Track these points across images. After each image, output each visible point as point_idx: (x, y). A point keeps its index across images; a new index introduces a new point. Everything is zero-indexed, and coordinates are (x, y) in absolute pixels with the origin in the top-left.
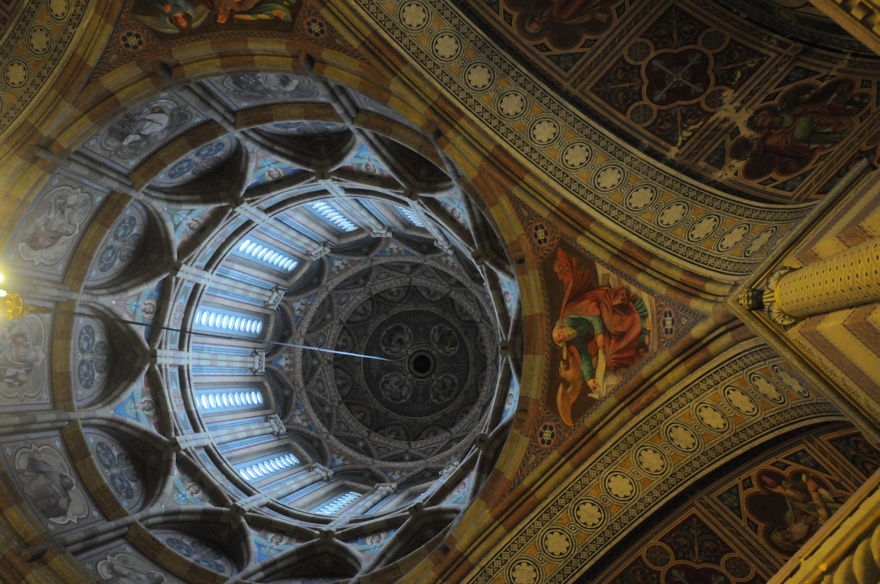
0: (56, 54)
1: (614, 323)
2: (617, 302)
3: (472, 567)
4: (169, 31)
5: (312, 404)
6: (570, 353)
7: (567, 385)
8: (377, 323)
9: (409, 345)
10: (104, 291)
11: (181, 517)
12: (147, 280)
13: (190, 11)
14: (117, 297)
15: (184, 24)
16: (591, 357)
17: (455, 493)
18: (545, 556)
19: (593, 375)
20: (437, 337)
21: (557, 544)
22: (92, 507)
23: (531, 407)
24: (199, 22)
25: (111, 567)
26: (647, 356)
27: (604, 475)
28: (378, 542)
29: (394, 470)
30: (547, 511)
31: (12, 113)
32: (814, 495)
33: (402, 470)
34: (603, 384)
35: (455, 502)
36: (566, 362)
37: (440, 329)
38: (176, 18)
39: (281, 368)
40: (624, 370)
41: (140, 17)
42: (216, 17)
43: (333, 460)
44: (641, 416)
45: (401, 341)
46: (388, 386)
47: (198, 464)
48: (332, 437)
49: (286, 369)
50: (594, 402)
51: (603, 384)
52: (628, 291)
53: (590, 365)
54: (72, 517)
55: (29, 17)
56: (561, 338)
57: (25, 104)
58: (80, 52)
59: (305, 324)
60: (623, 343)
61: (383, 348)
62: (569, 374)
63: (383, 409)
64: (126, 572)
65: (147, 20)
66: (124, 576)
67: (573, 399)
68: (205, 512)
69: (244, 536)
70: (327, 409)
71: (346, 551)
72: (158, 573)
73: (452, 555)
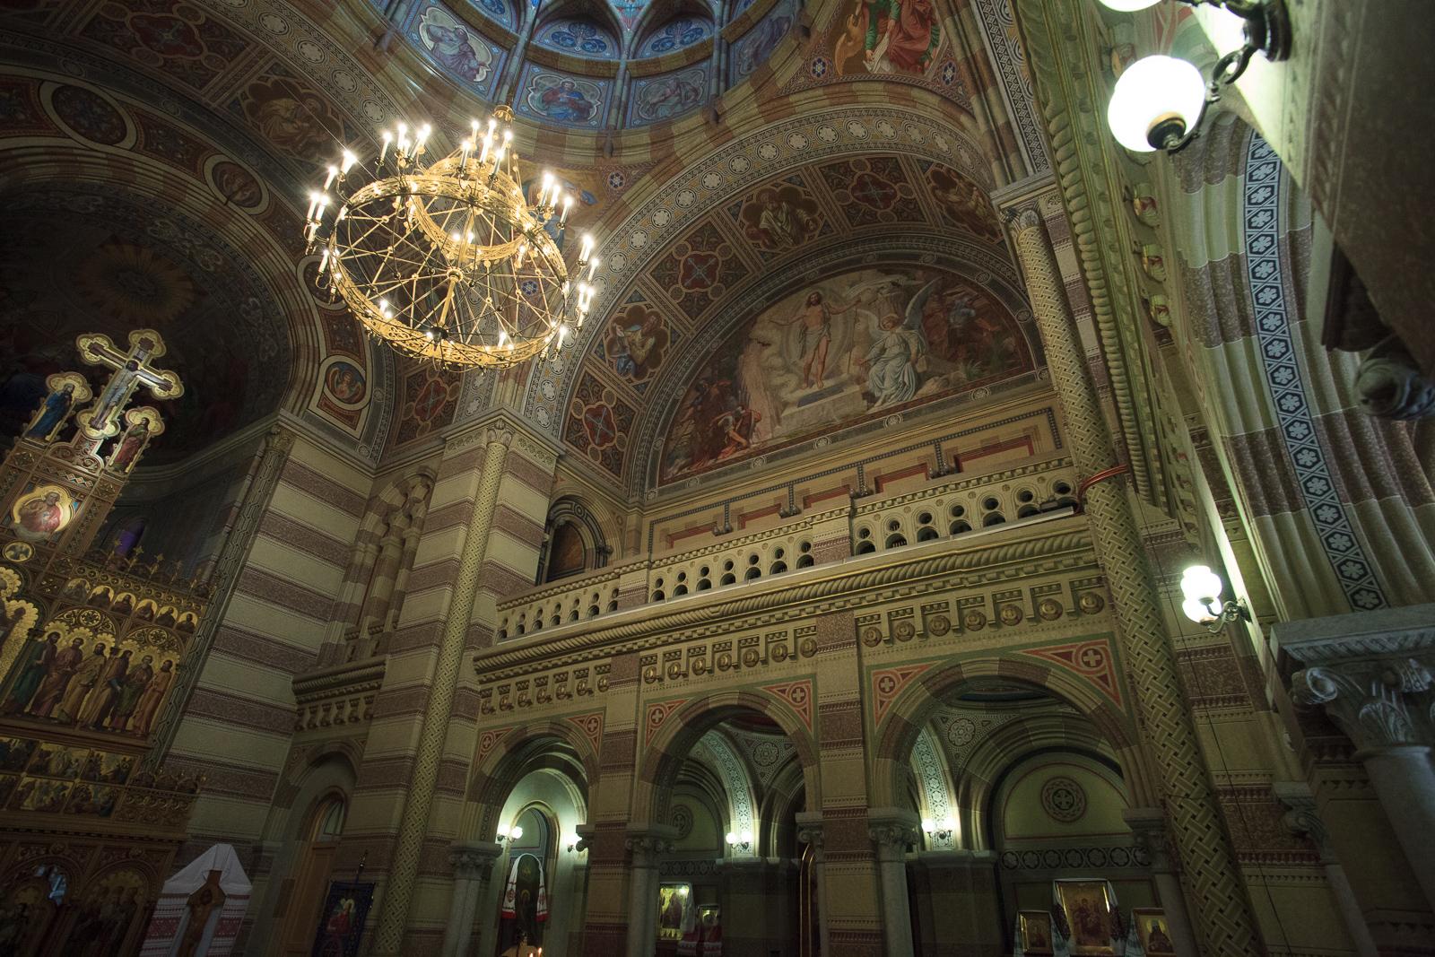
1: (909, 22)
2: (921, 8)
6: (862, 14)
16: (879, 32)
19: (873, 48)
21: (798, 142)
23: (814, 36)
25: (428, 31)
26: (919, 77)
32: (974, 197)
36: (856, 18)
44: (895, 107)
51: (877, 62)
52: (932, 11)
53: (875, 38)
60: (907, 45)
62: (855, 30)
64: (440, 34)
67: (850, 54)
72: (462, 28)
73: (721, 127)
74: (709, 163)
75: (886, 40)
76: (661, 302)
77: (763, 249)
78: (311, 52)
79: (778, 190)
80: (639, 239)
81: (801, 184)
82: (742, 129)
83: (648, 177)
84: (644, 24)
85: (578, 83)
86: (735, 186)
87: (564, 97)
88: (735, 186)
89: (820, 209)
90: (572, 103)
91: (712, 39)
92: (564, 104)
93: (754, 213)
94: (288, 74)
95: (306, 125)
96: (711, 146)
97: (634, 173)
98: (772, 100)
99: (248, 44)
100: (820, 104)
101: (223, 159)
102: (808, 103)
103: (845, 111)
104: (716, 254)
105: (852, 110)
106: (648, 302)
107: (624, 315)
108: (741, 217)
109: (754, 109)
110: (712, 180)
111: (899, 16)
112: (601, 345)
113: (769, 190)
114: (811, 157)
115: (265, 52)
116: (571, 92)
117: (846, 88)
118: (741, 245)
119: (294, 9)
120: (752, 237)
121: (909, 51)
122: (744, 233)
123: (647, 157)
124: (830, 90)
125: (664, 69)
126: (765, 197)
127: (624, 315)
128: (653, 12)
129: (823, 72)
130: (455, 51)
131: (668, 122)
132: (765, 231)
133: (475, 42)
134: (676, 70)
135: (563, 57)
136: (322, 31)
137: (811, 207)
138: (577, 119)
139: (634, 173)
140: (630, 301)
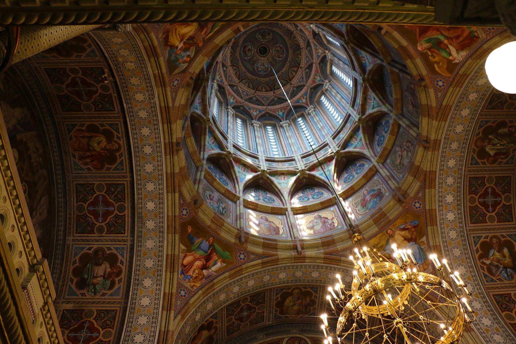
0: (154, 113)
3: (440, 140)
4: (185, 67)
5: (249, 102)
7: (438, 63)
8: (238, 53)
9: (253, 49)
10: (202, 153)
11: (292, 190)
12: (205, 134)
13: (188, 53)
14: (206, 150)
15: (188, 59)
17: (368, 104)
18: (463, 119)
19: (450, 54)
20: (260, 37)
21: (465, 112)
22: (277, 216)
23: (426, 78)
24: (193, 54)
27: (474, 82)
28: (356, 140)
29: (300, 99)
30: (457, 106)
31: (158, 145)
33: (302, 96)
34: (457, 56)
35: (373, 108)
36: (432, 56)
37: (259, 34)
38: (185, 61)
39: (233, 102)
40: (468, 48)
41: (173, 74)
42: (198, 46)
43: (279, 115)
45: (249, 50)
46: (259, 69)
47: (275, 169)
48: (269, 107)
49: (234, 101)
50: (457, 64)
51: (457, 56)
53: (447, 52)
54: (281, 227)
55: (131, 110)
56: (423, 49)
57: (159, 138)
58: (163, 105)
59: (224, 80)
60: (461, 39)
61: (246, 58)
62: (437, 59)
63: (267, 79)
65: (177, 71)
66: (313, 226)
67: (445, 66)
68: (295, 181)
69: (314, 176)
70: (254, 99)
71: (349, 152)
72: (316, 214)
73: (432, 142)
74: (443, 159)
75: (451, 47)
76: (490, 230)
77: (505, 161)
78: (282, 276)
79: (481, 135)
80: (451, 216)
81: (487, 122)
82: (440, 134)
83: (427, 190)
84: (368, 142)
85: (367, 187)
86: (462, 154)
87: (368, 197)
88: (462, 154)
89: (507, 120)
90: (373, 196)
91: (395, 120)
92: (371, 199)
93: (482, 154)
94: (282, 290)
95: (300, 301)
96: (436, 152)
97: (420, 195)
98: (438, 113)
99: (265, 292)
100: (456, 93)
101: (286, 340)
102: (451, 98)
103: (469, 82)
104: (488, 185)
105: (471, 79)
106: (484, 235)
107: (480, 252)
108: (479, 161)
109: (435, 123)
110: (452, 163)
111: (445, 36)
112: (486, 276)
113: (477, 140)
114: (477, 110)
115: (271, 289)
116: (368, 193)
117: (458, 76)
118: (494, 170)
119: (268, 268)
120: (494, 162)
121: (464, 40)
122: (488, 165)
123: (418, 184)
124: (454, 84)
125: (389, 148)
126: (479, 144)
127: (480, 252)
128: (366, 135)
129: (443, 82)
130: (321, 225)
131: (412, 164)
132: (496, 154)
133: (324, 214)
134: (394, 144)
135: (354, 185)
136: (280, 266)
137: (503, 124)
138: (380, 200)
139: (420, 195)
140: (476, 244)
